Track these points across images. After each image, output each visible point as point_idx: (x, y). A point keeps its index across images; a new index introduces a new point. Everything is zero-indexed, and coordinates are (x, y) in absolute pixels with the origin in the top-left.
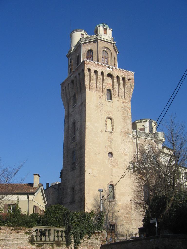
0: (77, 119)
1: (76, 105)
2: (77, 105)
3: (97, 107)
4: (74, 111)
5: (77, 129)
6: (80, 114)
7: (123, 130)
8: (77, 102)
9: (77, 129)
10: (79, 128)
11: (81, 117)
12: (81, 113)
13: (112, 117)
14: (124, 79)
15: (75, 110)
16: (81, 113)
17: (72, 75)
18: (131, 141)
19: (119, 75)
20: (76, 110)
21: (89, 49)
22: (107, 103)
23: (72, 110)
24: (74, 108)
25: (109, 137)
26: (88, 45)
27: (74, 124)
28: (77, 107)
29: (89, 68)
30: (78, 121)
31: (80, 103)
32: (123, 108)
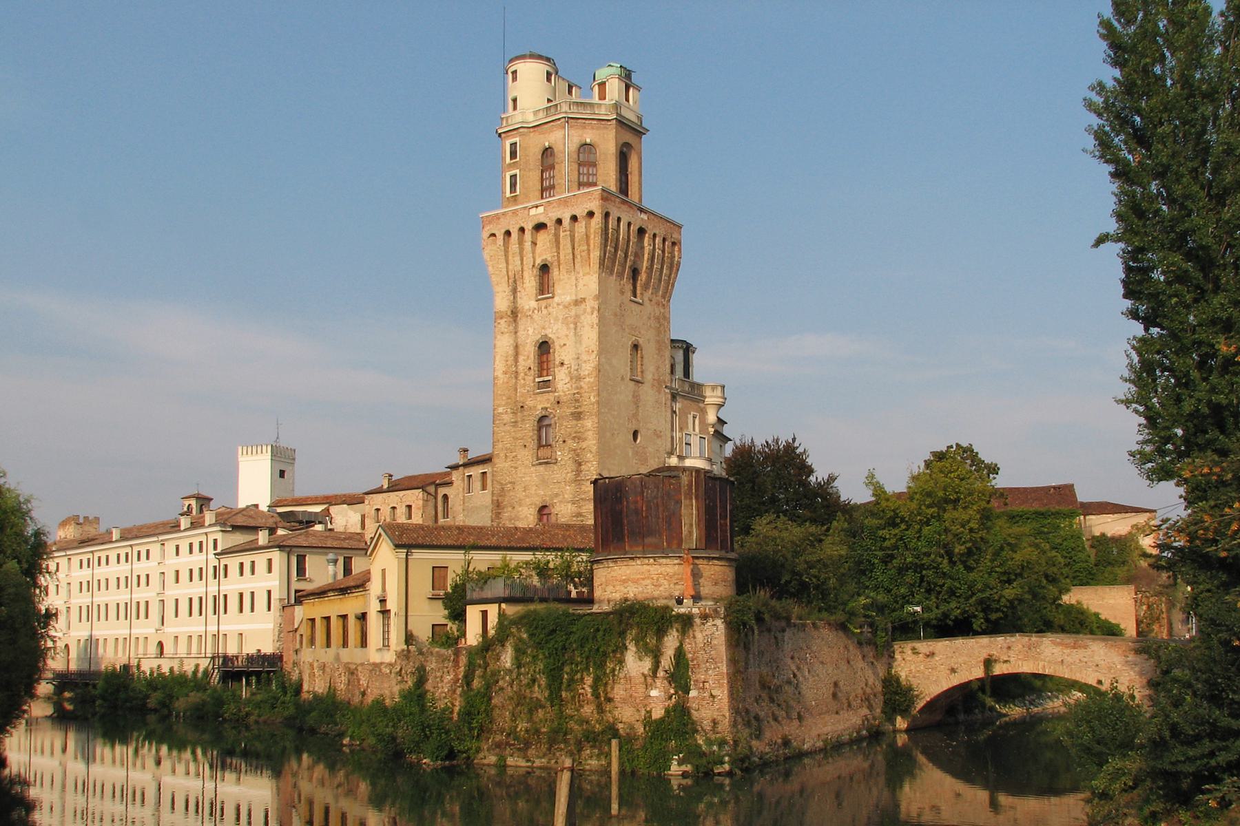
0: (558, 338)
1: (553, 298)
2: (556, 299)
3: (616, 315)
4: (545, 312)
5: (557, 363)
6: (572, 326)
7: (656, 377)
8: (558, 290)
9: (557, 363)
10: (566, 362)
11: (575, 334)
12: (576, 324)
13: (641, 341)
14: (664, 240)
15: (546, 307)
16: (576, 324)
17: (537, 207)
18: (669, 403)
19: (657, 232)
20: (550, 309)
21: (588, 141)
22: (634, 306)
23: (533, 304)
24: (544, 303)
25: (634, 392)
26: (585, 128)
27: (544, 347)
28: (558, 304)
29: (609, 210)
30: (565, 345)
31: (574, 298)
32: (657, 319)
